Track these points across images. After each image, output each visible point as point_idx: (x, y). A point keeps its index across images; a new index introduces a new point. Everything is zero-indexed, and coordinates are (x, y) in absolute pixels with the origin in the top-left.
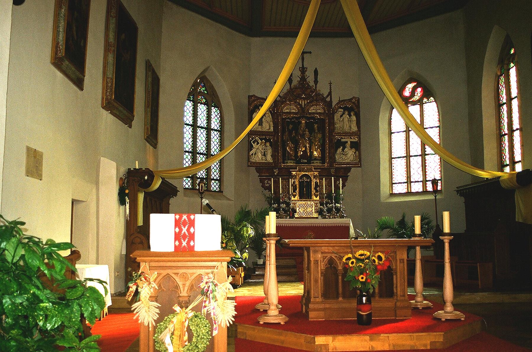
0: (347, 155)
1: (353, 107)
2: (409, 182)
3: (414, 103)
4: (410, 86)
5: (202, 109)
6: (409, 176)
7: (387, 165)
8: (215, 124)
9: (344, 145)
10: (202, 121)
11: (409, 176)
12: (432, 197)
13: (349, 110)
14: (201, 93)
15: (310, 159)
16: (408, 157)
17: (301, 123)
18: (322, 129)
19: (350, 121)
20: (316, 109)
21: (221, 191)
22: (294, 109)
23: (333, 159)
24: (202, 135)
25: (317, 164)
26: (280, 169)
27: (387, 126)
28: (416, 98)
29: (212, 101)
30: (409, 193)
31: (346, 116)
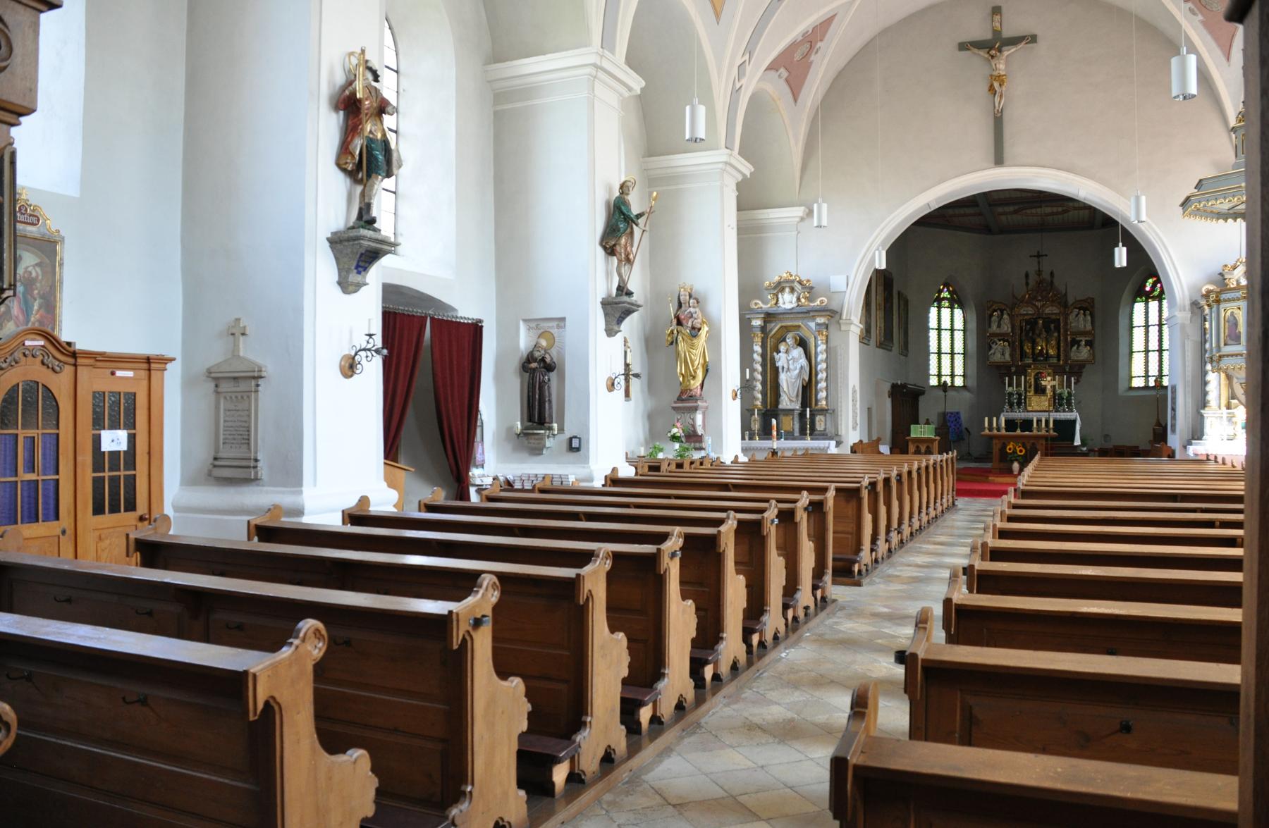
0: (1084, 353)
1: (1086, 306)
2: (1147, 376)
3: (1154, 298)
4: (1151, 281)
5: (946, 312)
6: (1147, 371)
7: (1126, 359)
8: (959, 324)
9: (1078, 343)
10: (946, 324)
11: (1147, 371)
12: (1153, 393)
13: (1085, 309)
14: (944, 299)
15: (1048, 356)
16: (1147, 351)
17: (1036, 323)
18: (1058, 329)
19: (1085, 321)
20: (1051, 310)
21: (964, 386)
22: (1030, 311)
23: (1067, 357)
24: (946, 336)
25: (1055, 361)
26: (1017, 366)
27: (1127, 321)
28: (1156, 293)
29: (956, 301)
30: (1147, 387)
31: (1081, 317)
